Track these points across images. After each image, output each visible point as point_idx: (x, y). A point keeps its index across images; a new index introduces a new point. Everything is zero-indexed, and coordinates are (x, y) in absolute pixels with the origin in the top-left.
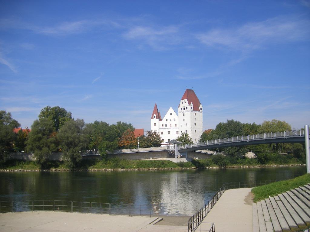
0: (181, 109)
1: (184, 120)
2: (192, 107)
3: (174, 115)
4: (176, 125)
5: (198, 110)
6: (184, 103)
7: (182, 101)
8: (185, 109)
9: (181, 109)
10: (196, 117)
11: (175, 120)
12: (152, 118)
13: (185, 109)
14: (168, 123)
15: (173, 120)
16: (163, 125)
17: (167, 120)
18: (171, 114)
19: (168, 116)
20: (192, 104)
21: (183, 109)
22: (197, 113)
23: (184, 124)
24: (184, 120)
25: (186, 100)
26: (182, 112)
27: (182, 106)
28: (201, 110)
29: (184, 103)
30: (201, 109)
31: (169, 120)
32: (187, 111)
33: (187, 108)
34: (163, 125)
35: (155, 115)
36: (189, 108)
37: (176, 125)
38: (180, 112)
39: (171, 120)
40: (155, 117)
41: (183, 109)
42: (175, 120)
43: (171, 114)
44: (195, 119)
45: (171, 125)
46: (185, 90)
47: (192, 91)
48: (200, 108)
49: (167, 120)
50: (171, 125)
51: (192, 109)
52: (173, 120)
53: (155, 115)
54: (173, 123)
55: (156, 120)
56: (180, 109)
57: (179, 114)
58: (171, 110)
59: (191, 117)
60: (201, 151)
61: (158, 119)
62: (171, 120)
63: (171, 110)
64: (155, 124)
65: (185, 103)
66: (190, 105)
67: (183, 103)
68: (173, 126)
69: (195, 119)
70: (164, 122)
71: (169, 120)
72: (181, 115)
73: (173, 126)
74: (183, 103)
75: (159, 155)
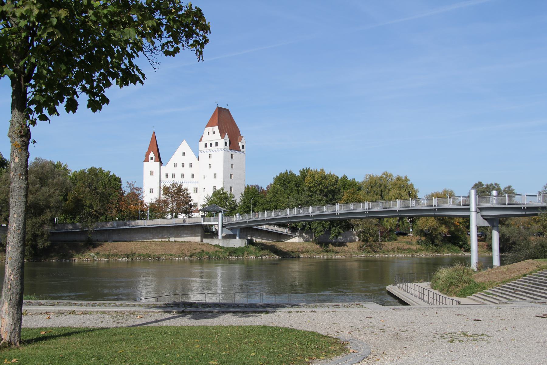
0: (206, 145)
1: (210, 166)
2: (226, 143)
3: (191, 156)
4: (193, 176)
5: (238, 149)
6: (211, 133)
7: (207, 130)
8: (214, 144)
9: (206, 145)
10: (232, 162)
11: (191, 165)
12: (147, 160)
13: (214, 144)
14: (178, 171)
15: (187, 165)
16: (167, 176)
17: (175, 165)
18: (184, 154)
19: (177, 157)
20: (227, 137)
21: (208, 145)
22: (236, 154)
23: (210, 174)
24: (210, 166)
25: (216, 129)
26: (206, 151)
27: (207, 139)
28: (243, 148)
29: (211, 133)
30: (243, 146)
31: (179, 165)
32: (217, 150)
34: (167, 176)
35: (152, 155)
36: (221, 143)
37: (193, 176)
39: (183, 165)
40: (152, 159)
41: (208, 145)
42: (191, 165)
43: (184, 154)
44: (232, 165)
45: (183, 176)
46: (215, 108)
47: (228, 110)
48: (240, 144)
49: (175, 165)
50: (183, 176)
51: (226, 145)
52: (187, 165)
53: (152, 155)
54: (187, 171)
55: (153, 165)
56: (202, 144)
57: (200, 155)
58: (184, 146)
59: (224, 162)
60: (264, 226)
61: (158, 163)
62: (183, 165)
63: (184, 146)
64: (152, 173)
65: (213, 134)
66: (222, 137)
67: (209, 133)
68: (188, 177)
69: (232, 165)
70: (168, 169)
71: (179, 165)
72: (204, 156)
73: (188, 177)
74: (209, 133)
75: (186, 232)
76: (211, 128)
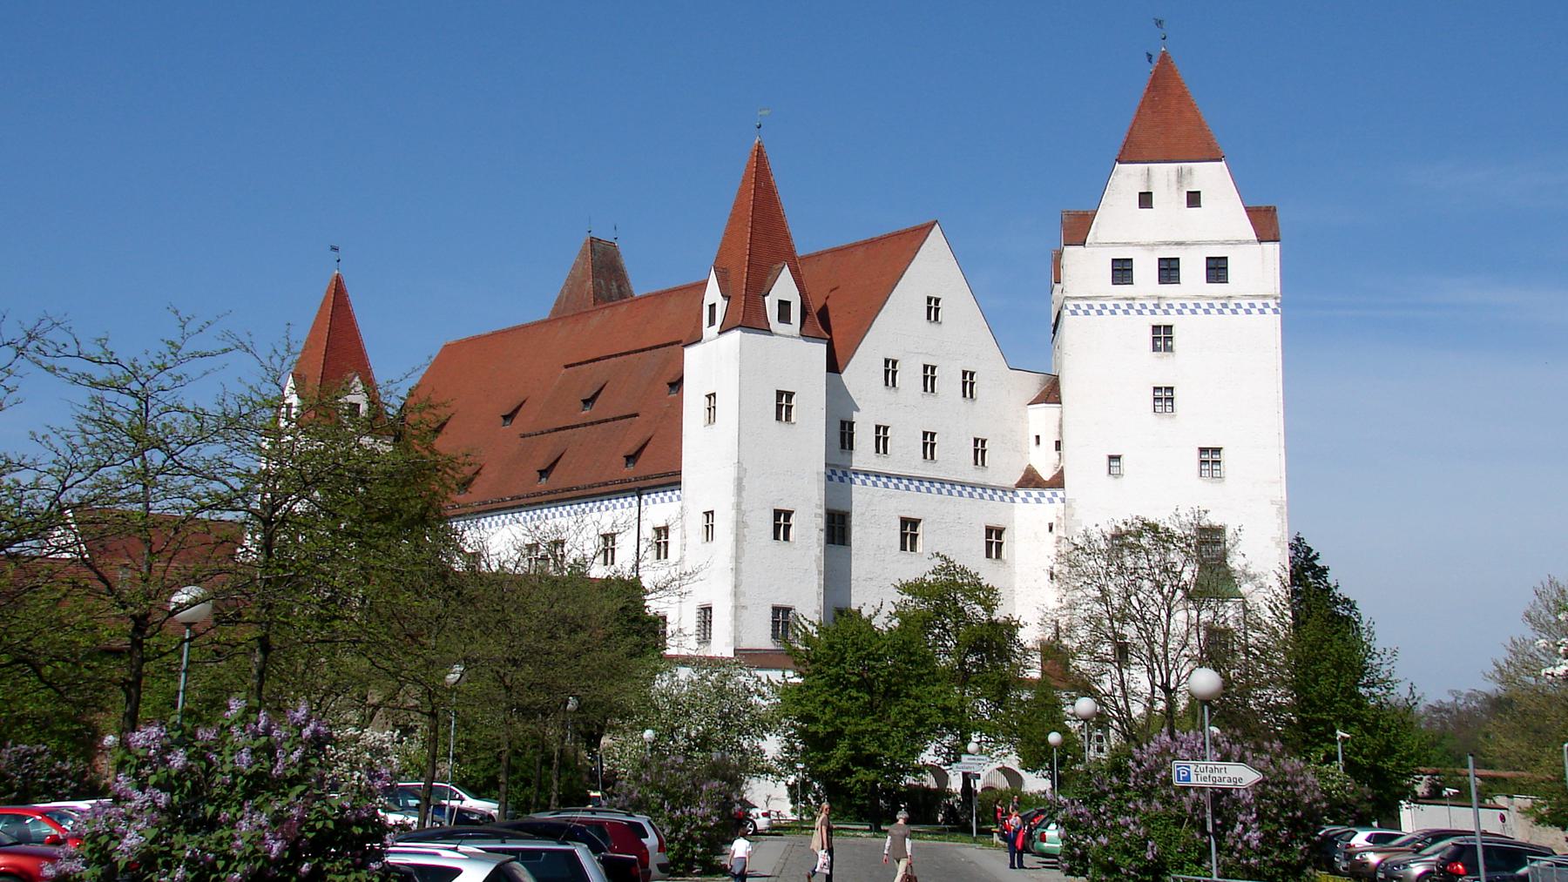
0: (1122, 271)
1: (1164, 397)
4: (980, 449)
7: (1128, 178)
9: (1122, 271)
15: (949, 382)
17: (890, 369)
18: (933, 308)
19: (895, 328)
24: (1164, 397)
31: (909, 376)
33: (1217, 269)
37: (980, 449)
38: (1092, 305)
43: (933, 308)
45: (929, 442)
50: (929, 442)
52: (949, 382)
56: (1085, 269)
67: (1145, 200)
71: (909, 376)
74: (1145, 200)
76: (1163, 172)
